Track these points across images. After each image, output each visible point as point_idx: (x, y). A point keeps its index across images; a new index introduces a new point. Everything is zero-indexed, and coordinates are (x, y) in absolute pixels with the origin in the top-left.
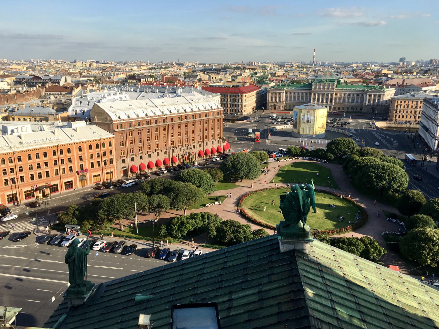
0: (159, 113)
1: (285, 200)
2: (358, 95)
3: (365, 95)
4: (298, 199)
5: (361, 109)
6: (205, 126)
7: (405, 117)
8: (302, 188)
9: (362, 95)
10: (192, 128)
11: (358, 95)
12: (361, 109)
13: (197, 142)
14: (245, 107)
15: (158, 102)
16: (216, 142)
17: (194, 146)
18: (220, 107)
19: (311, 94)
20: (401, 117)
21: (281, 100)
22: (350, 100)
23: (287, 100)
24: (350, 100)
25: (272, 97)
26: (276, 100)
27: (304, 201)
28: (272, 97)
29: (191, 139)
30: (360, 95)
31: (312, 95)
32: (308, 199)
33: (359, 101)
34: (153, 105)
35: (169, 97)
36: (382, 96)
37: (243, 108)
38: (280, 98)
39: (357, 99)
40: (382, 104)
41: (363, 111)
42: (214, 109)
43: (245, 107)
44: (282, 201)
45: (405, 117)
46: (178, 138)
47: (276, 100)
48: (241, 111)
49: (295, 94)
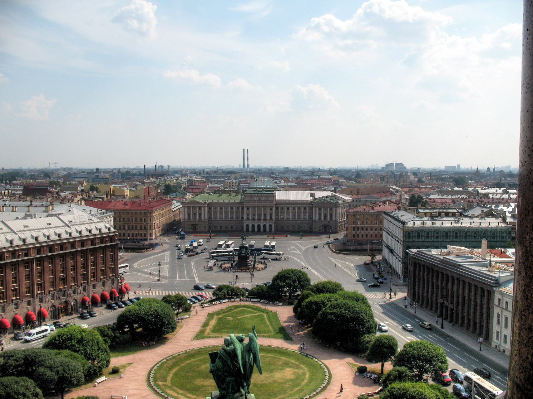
0: (17, 242)
1: (217, 360)
4: (236, 355)
5: (311, 228)
6: (91, 258)
7: (365, 236)
8: (241, 340)
9: (311, 208)
10: (71, 262)
11: (305, 209)
13: (79, 284)
14: (150, 229)
15: (17, 225)
16: (109, 283)
17: (74, 293)
18: (112, 230)
19: (243, 208)
20: (360, 236)
21: (203, 218)
25: (189, 214)
26: (195, 218)
27: (243, 358)
29: (70, 279)
31: (245, 209)
32: (250, 355)
34: (8, 230)
35: (35, 217)
37: (147, 231)
38: (200, 214)
39: (305, 215)
41: (314, 230)
42: (105, 233)
43: (150, 229)
44: (213, 362)
45: (365, 236)
46: (49, 277)
47: (195, 218)
48: (145, 235)
49: (221, 208)
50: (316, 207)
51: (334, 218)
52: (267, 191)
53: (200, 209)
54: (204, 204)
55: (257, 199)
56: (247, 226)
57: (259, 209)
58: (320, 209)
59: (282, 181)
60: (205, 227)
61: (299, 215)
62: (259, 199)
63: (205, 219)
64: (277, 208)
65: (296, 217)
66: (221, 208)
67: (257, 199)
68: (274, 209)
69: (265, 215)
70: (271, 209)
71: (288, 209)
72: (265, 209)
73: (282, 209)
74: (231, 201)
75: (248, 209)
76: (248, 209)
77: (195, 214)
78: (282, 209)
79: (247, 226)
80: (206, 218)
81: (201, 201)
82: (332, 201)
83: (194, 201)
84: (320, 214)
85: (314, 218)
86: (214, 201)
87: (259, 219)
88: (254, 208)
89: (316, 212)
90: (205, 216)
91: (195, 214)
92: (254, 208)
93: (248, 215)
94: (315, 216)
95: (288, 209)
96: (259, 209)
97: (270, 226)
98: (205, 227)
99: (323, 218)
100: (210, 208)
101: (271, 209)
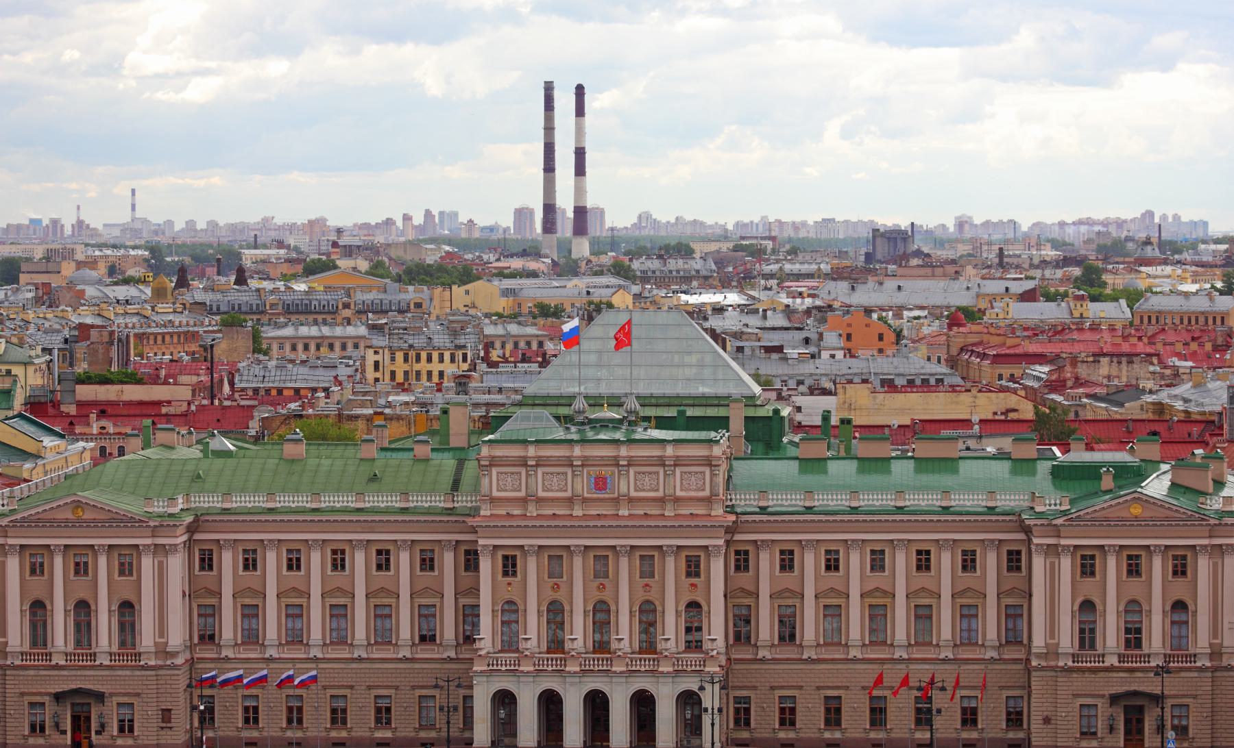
2: (969, 562)
3: (1038, 563)
5: (1015, 718)
9: (1014, 561)
11: (969, 562)
12: (1015, 718)
19: (471, 560)
21: (147, 639)
22: (901, 626)
23: (209, 638)
24: (901, 626)
25: (38, 609)
28: (38, 609)
30: (991, 563)
31: (485, 565)
33: (991, 626)
36: (1203, 565)
38: (127, 609)
39: (968, 613)
40: (1216, 653)
49: (294, 564)
50: (1052, 551)
51: (1202, 641)
52: (662, 423)
53: (127, 567)
54: (166, 523)
55: (582, 485)
56: (505, 700)
57: (602, 560)
58: (1087, 566)
59: (831, 338)
60: (166, 715)
61: (923, 616)
62: (600, 483)
63: (163, 651)
64: (742, 561)
65: (901, 635)
66: (294, 564)
67: (582, 485)
68: (717, 568)
69: (602, 615)
70: (693, 568)
71: (832, 565)
72: (648, 562)
73: (787, 562)
74: (370, 502)
75: (509, 566)
76: (509, 566)
77: (83, 609)
78: (787, 562)
79: (505, 700)
80: (177, 636)
81: (130, 505)
82: (1184, 502)
83: (78, 505)
84: (1087, 606)
85: (1039, 641)
86: (238, 502)
87: (602, 647)
88: (556, 560)
89: (1053, 587)
90: (167, 624)
91: (83, 609)
92: (556, 560)
93: (510, 611)
94: (1052, 628)
95: (832, 565)
96: (602, 560)
97: (688, 700)
98: (166, 715)
99: (1111, 636)
100: (207, 562)
101: (693, 568)
